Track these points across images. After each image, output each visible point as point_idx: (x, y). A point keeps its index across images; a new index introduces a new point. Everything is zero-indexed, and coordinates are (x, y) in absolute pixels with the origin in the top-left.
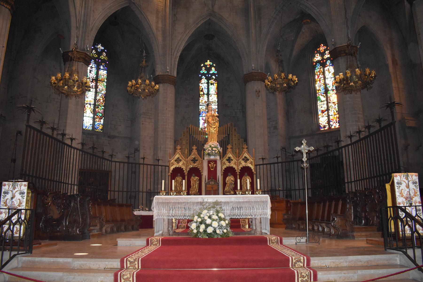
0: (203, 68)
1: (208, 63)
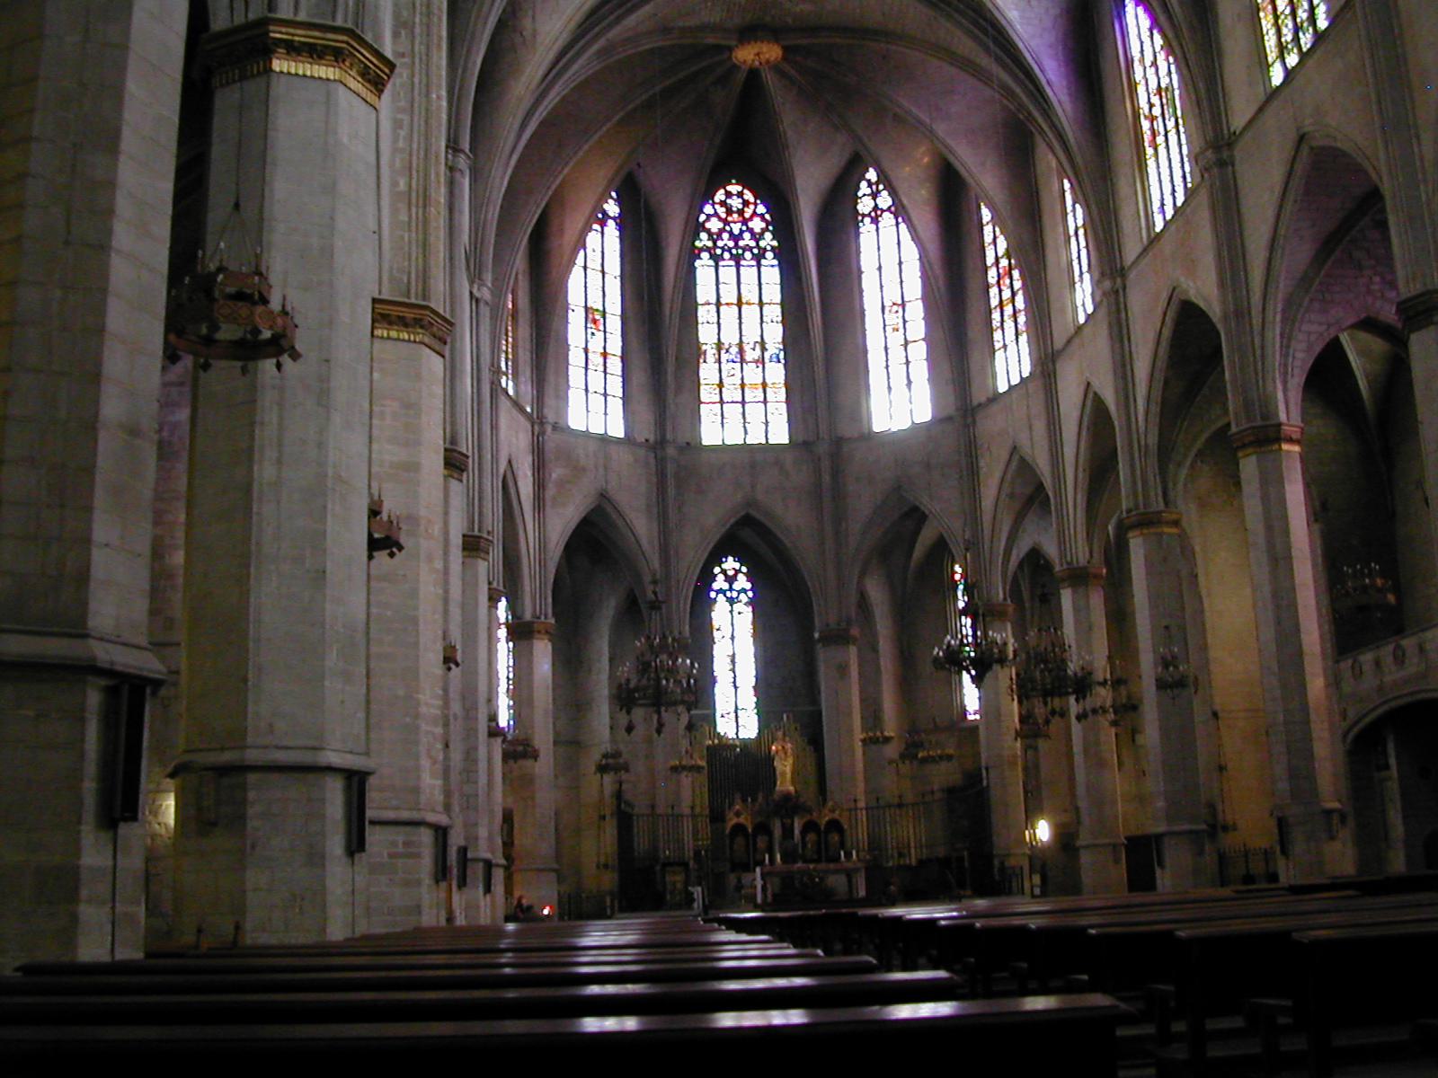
0: (721, 578)
1: (730, 564)
